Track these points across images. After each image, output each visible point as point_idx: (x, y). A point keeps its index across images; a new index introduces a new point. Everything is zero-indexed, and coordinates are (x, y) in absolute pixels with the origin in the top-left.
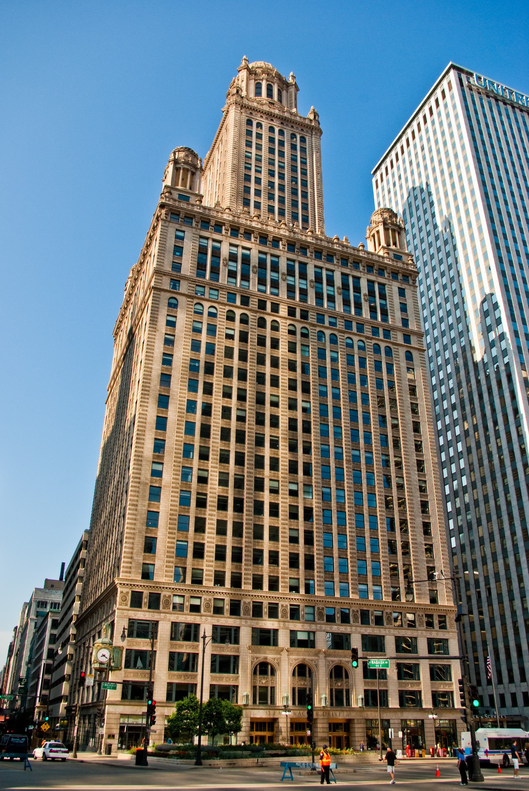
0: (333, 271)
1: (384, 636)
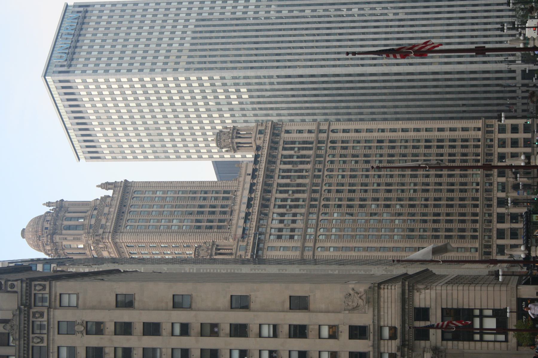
0: (280, 169)
1: (498, 153)
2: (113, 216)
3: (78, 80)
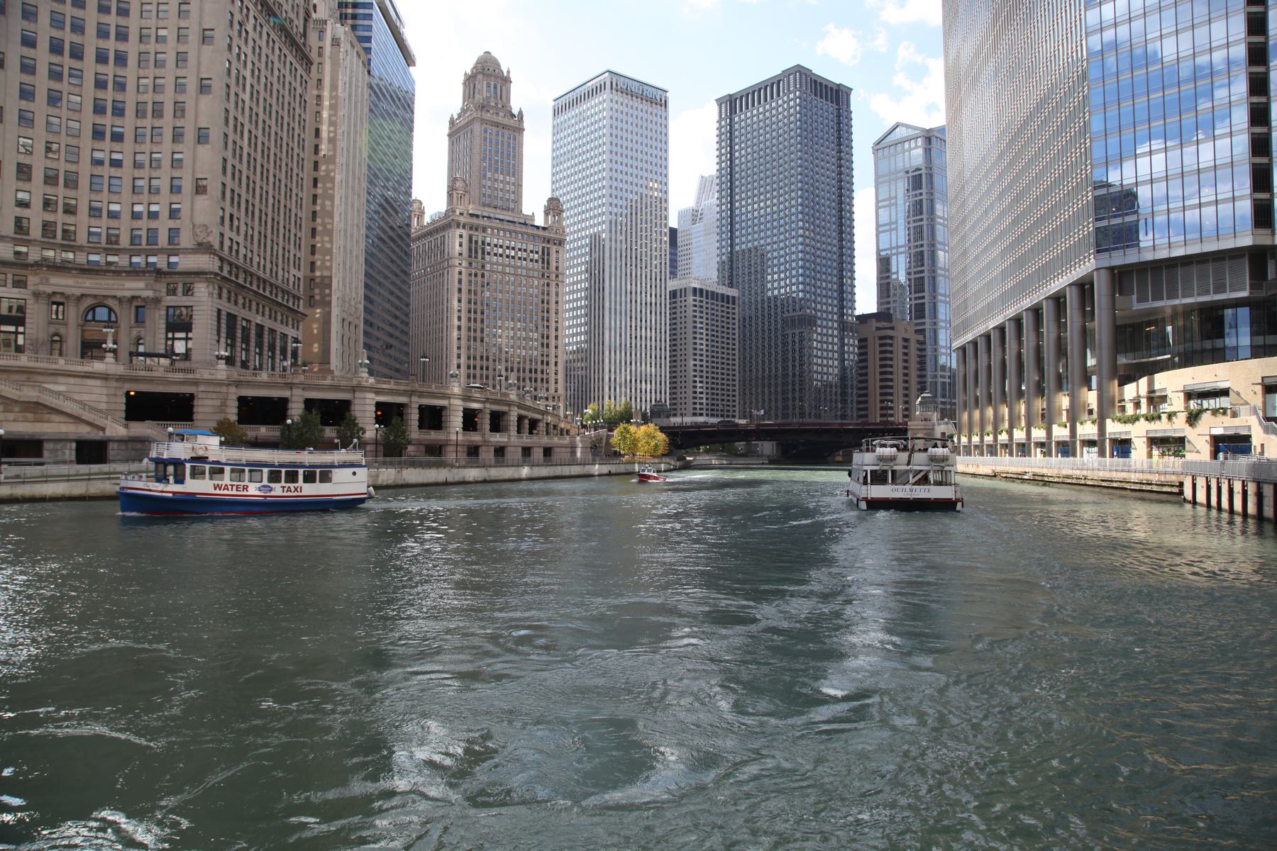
2: (495, 118)
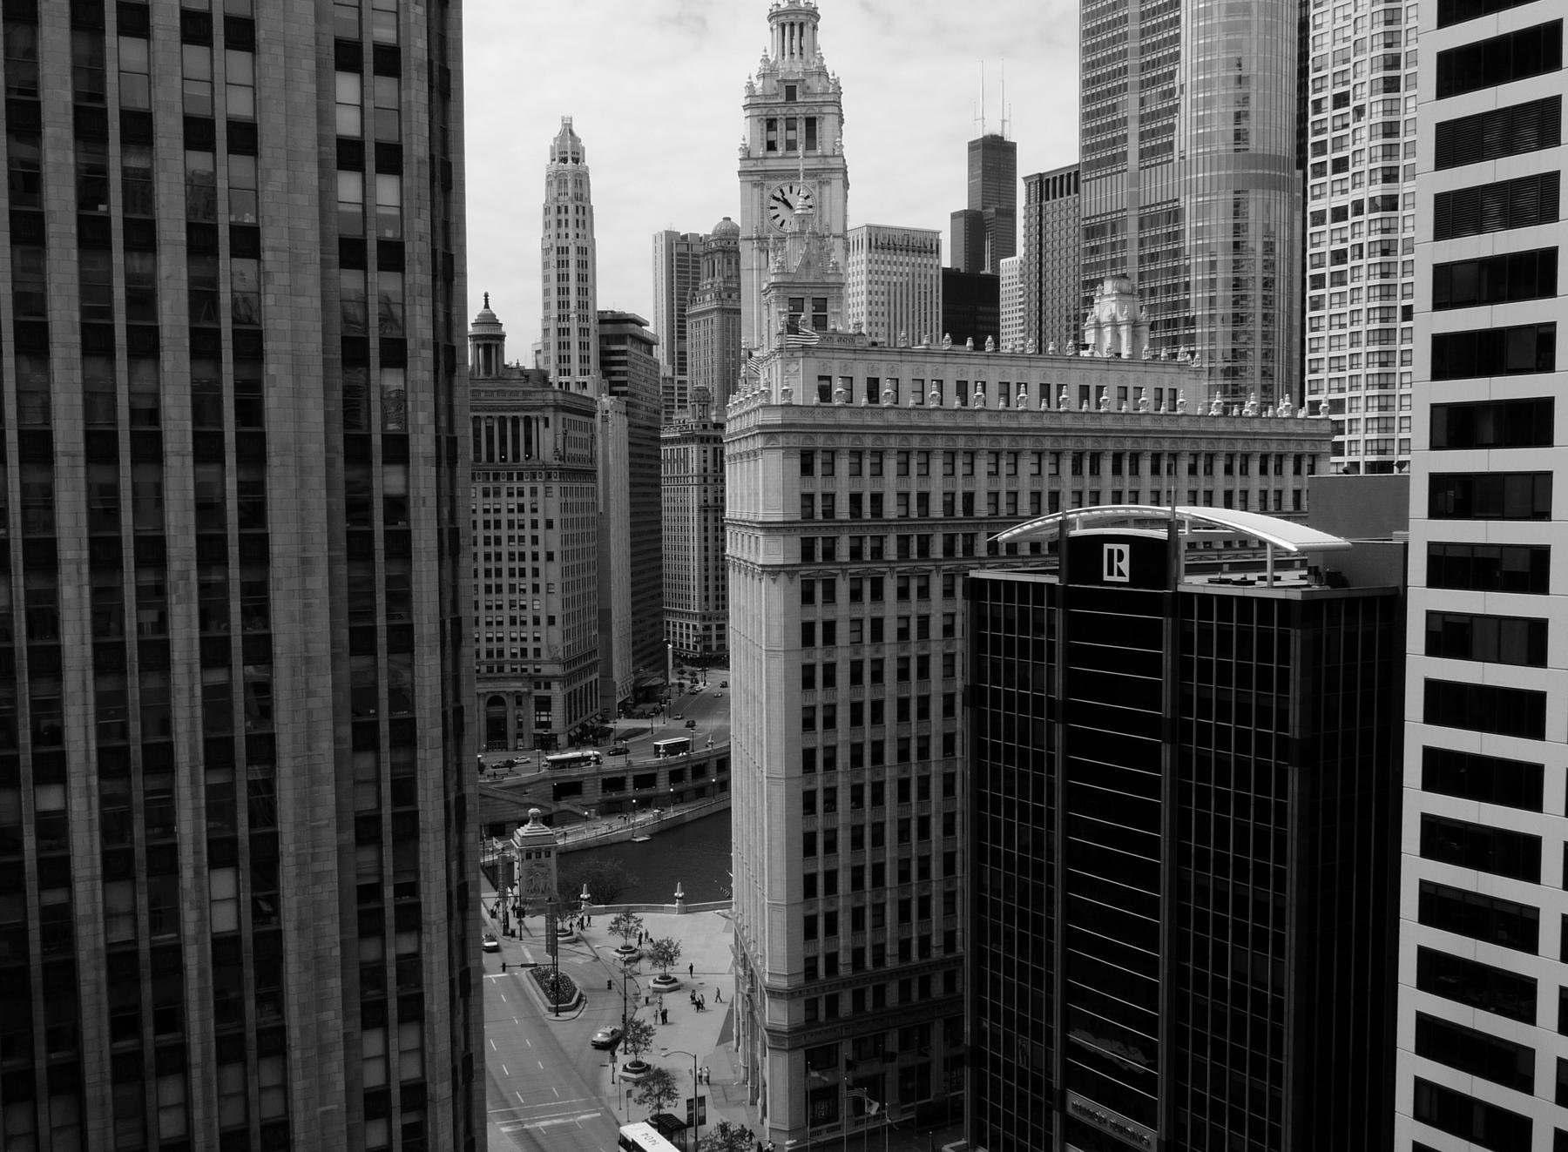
3: (864, 257)
